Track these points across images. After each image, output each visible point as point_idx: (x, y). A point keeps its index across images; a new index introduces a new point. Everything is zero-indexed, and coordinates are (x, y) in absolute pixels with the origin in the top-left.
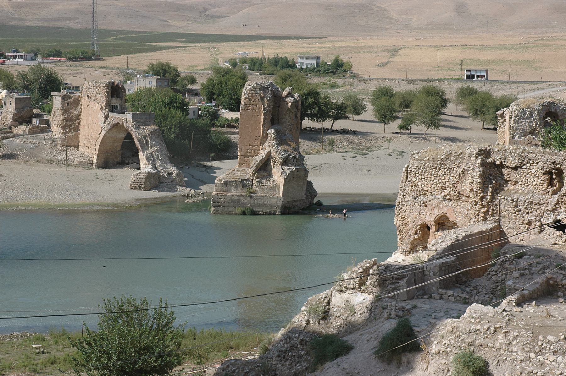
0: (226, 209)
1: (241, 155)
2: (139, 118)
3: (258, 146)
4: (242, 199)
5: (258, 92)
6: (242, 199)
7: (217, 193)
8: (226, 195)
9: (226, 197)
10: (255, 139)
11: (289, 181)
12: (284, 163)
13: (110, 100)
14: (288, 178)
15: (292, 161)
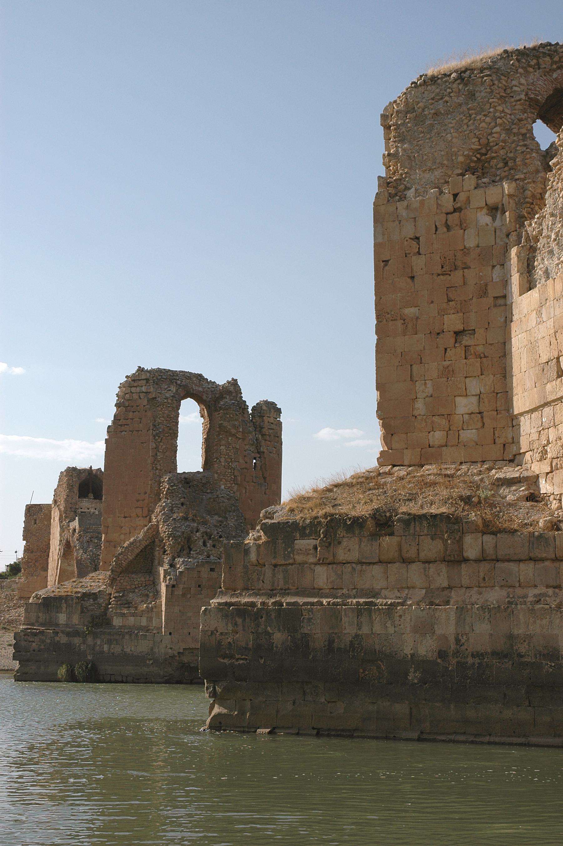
0: (42, 668)
1: (108, 542)
2: (94, 525)
3: (143, 517)
4: (77, 641)
5: (144, 389)
6: (77, 641)
7: (26, 627)
8: (42, 632)
9: (43, 638)
10: (138, 501)
11: (184, 595)
12: (185, 552)
13: (74, 501)
14: (181, 586)
15: (201, 543)
